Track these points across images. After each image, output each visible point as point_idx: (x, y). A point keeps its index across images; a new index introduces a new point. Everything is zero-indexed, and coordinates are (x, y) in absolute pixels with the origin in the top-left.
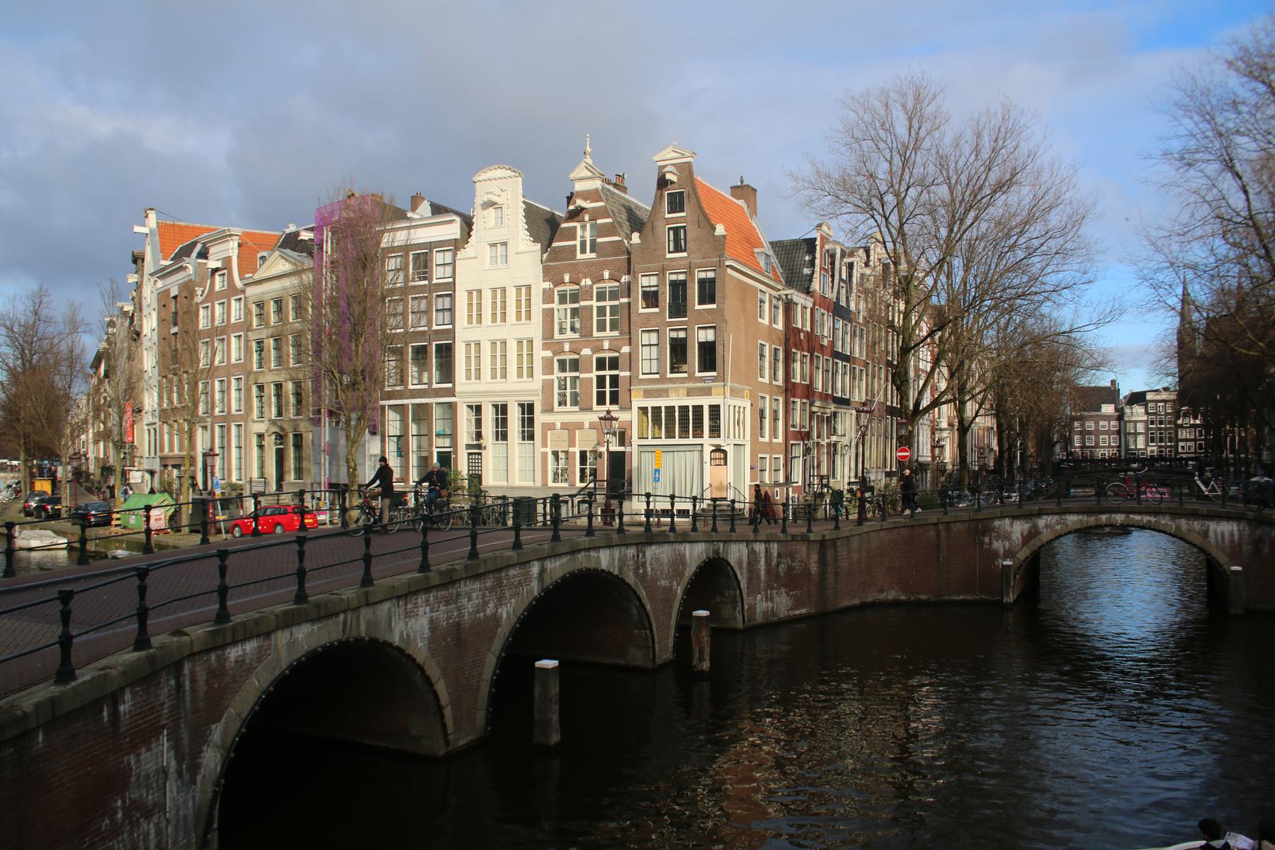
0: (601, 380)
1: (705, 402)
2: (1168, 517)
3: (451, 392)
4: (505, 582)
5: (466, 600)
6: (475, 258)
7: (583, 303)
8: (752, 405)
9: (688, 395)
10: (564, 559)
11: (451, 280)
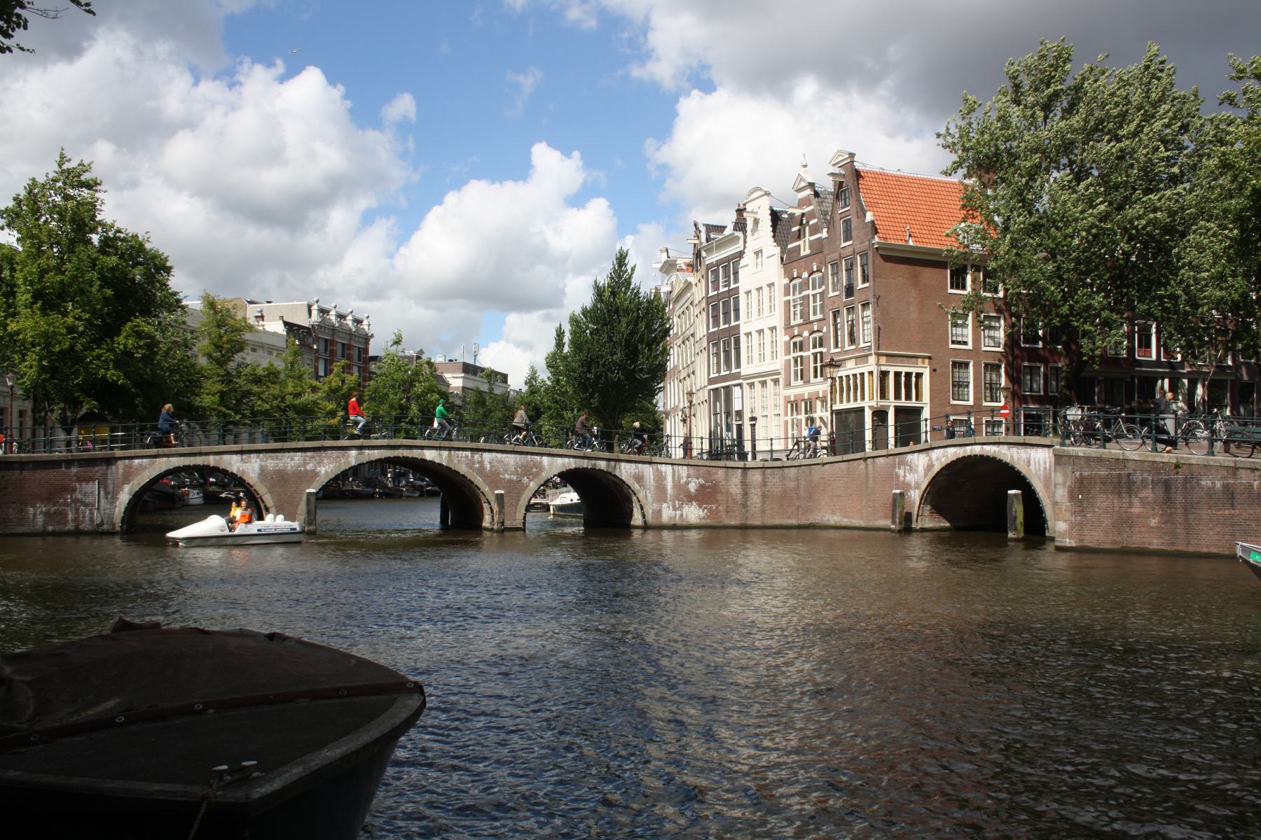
0: (815, 355)
1: (865, 370)
2: (1006, 447)
3: (737, 376)
7: (805, 293)
8: (935, 370)
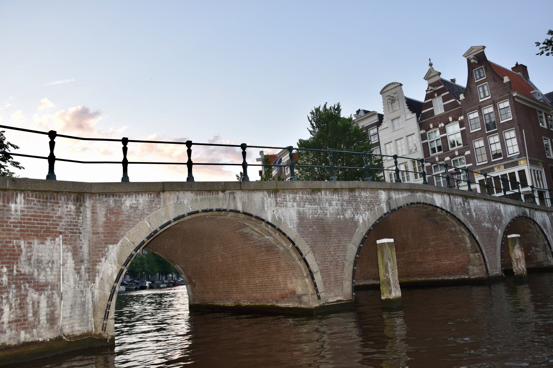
4: (359, 199)
5: (327, 204)
6: (387, 127)
9: (505, 168)
10: (406, 194)
11: (378, 141)
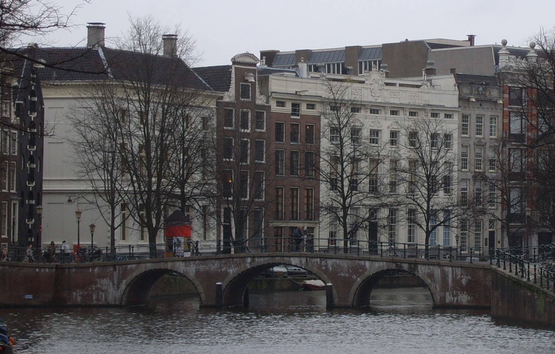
10: (266, 259)
